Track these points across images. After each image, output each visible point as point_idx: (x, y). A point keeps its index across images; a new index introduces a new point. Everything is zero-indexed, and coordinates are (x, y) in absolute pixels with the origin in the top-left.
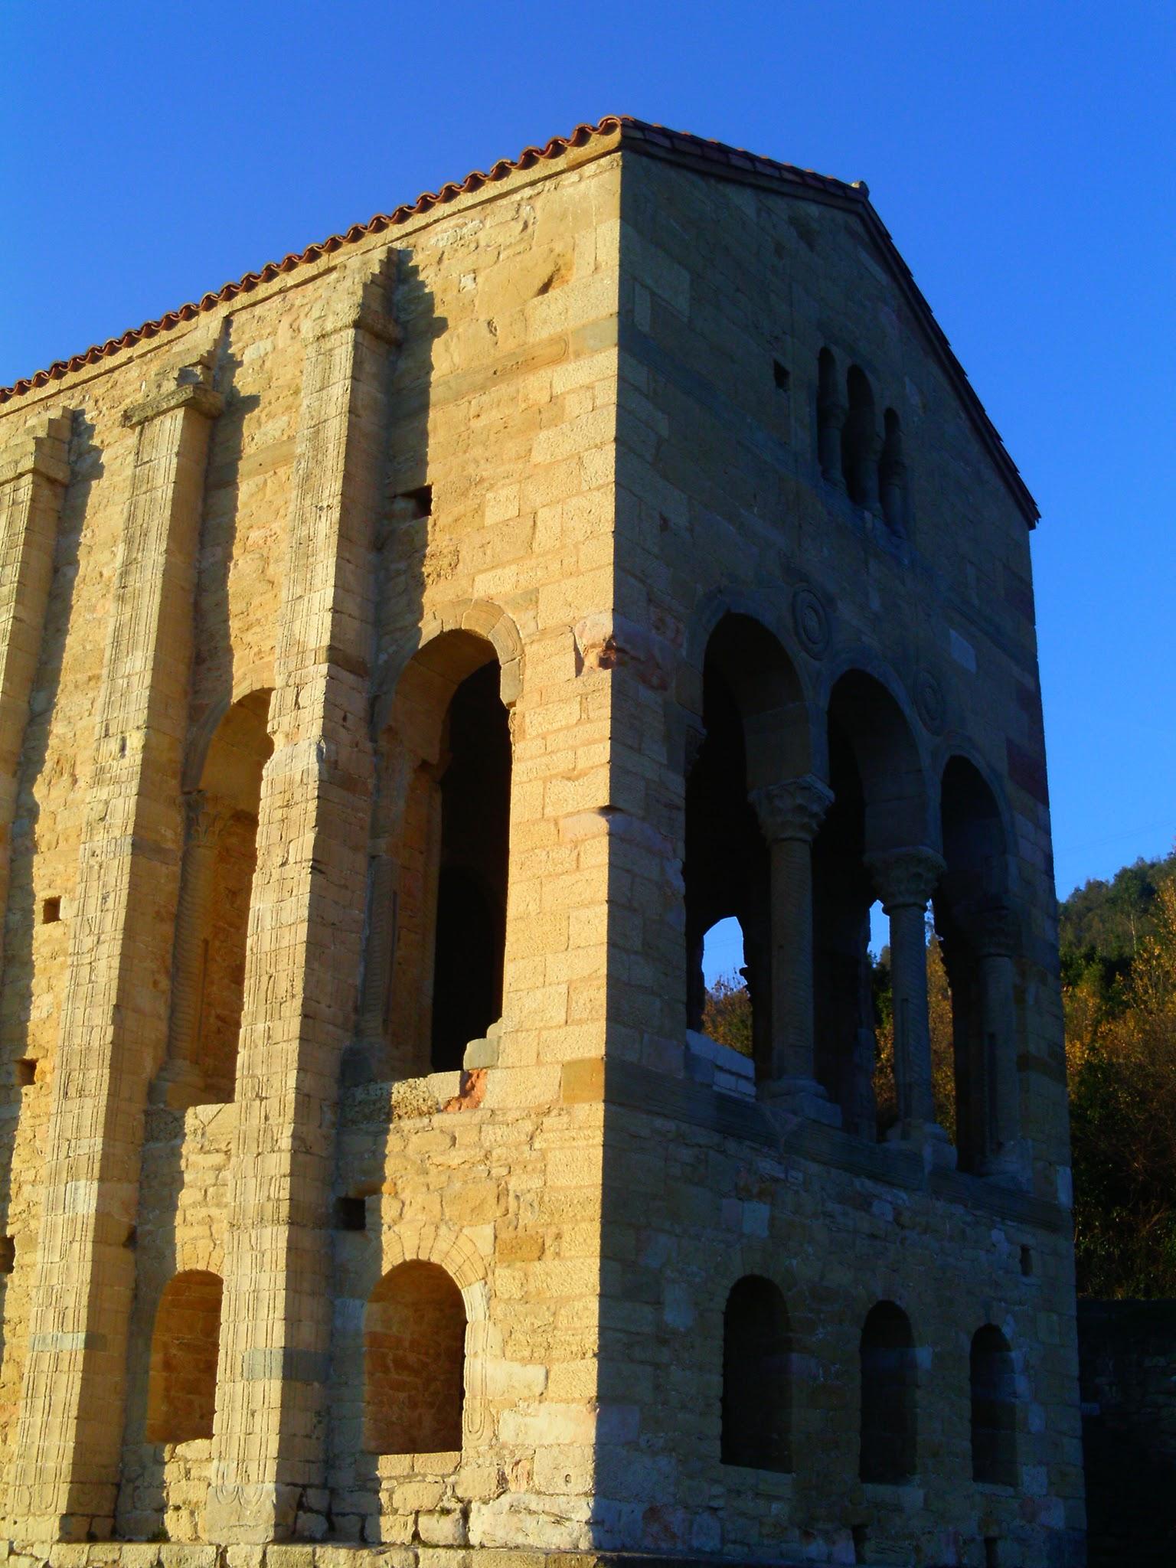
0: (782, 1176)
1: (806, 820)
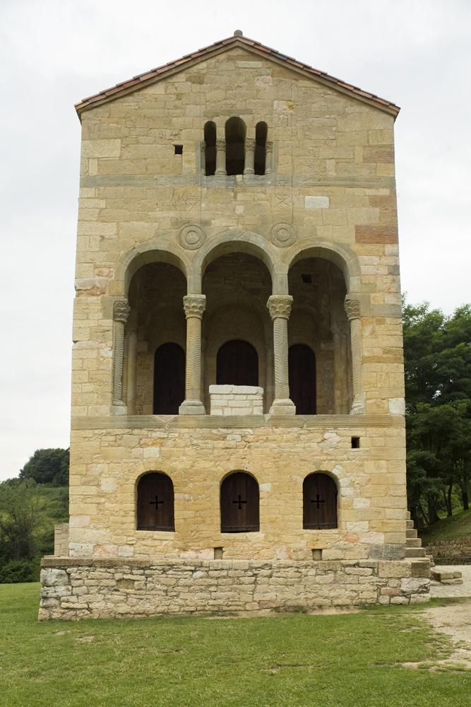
0: (166, 436)
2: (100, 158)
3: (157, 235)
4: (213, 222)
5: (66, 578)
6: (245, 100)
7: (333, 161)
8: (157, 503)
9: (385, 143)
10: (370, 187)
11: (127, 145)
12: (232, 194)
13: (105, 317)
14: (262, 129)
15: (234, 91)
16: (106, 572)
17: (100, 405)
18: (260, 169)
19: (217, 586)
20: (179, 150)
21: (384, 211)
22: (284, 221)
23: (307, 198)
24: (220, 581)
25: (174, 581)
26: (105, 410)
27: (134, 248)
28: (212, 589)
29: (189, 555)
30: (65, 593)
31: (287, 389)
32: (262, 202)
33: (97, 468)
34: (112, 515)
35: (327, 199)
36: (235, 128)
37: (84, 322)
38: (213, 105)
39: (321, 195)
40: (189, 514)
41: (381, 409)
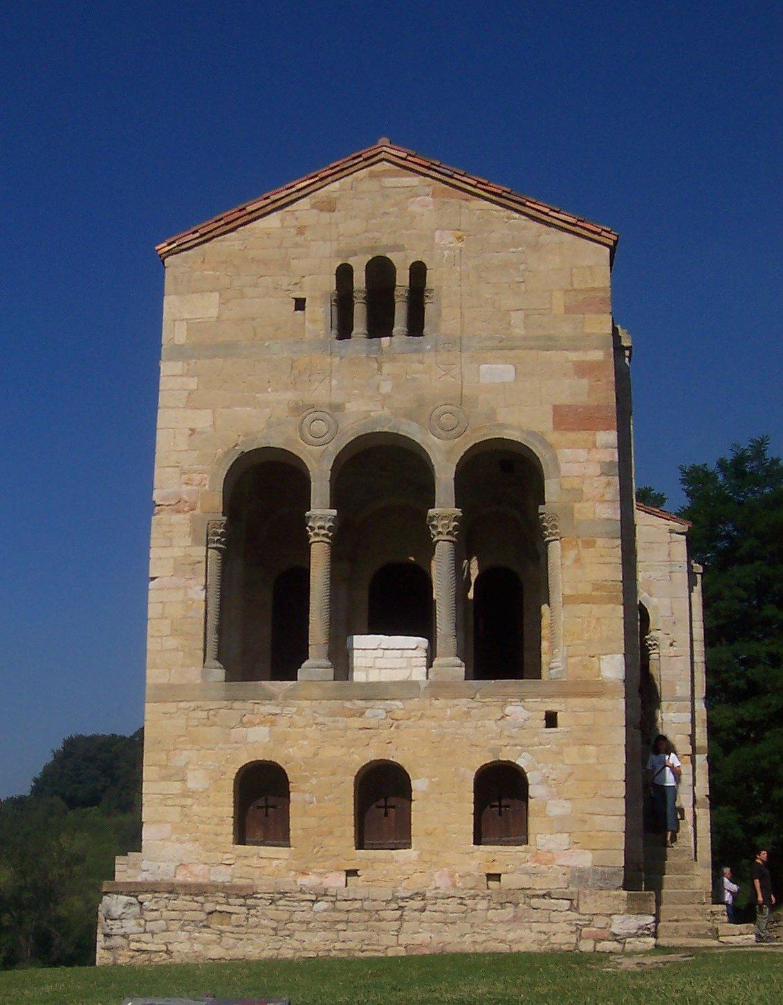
2: (190, 319)
3: (269, 425)
4: (348, 405)
5: (136, 909)
6: (395, 232)
7: (520, 313)
8: (267, 807)
9: (596, 285)
10: (575, 349)
11: (229, 300)
12: (375, 365)
13: (196, 542)
14: (418, 271)
15: (379, 219)
16: (193, 900)
18: (416, 327)
19: (347, 922)
20: (300, 304)
21: (595, 383)
22: (449, 402)
23: (483, 367)
24: (352, 916)
25: (286, 916)
26: (194, 674)
27: (236, 445)
28: (340, 926)
29: (310, 880)
30: (136, 929)
31: (452, 642)
32: (418, 376)
33: (180, 759)
34: (202, 822)
35: (511, 367)
36: (380, 269)
39: (502, 364)
40: (312, 822)
41: (588, 671)
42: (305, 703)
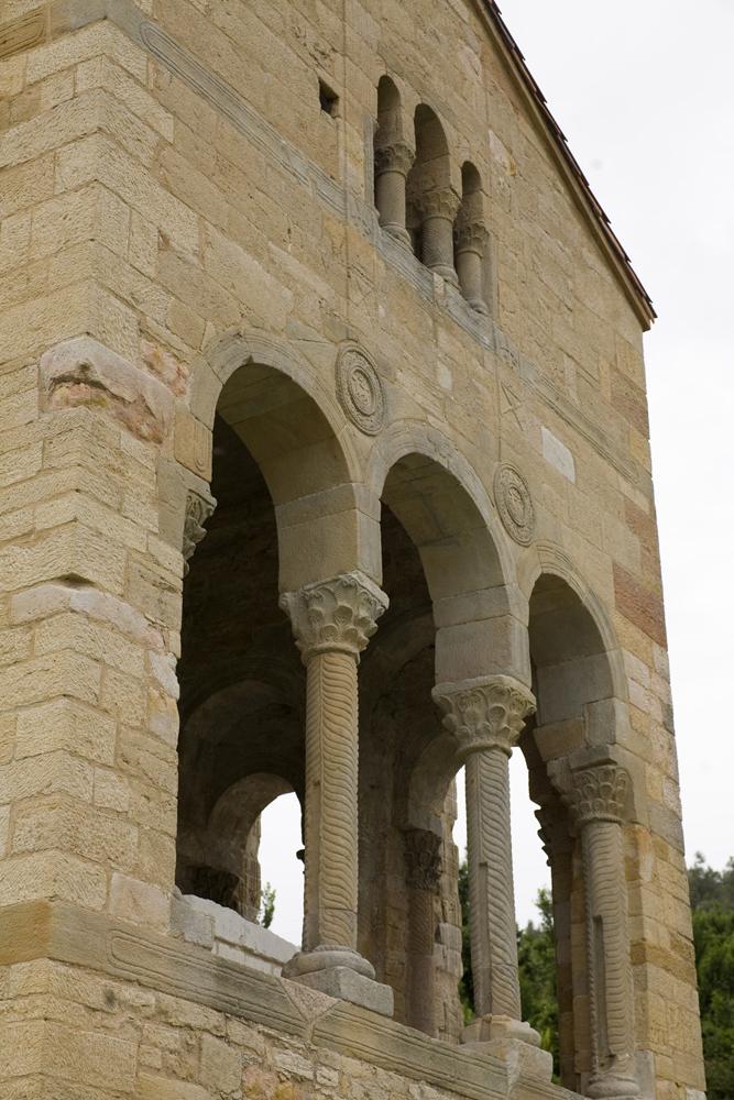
0: (309, 1074)
1: (351, 627)
10: (626, 476)
17: (148, 880)
37: (114, 519)
38: (395, 39)
42: (353, 1066)
